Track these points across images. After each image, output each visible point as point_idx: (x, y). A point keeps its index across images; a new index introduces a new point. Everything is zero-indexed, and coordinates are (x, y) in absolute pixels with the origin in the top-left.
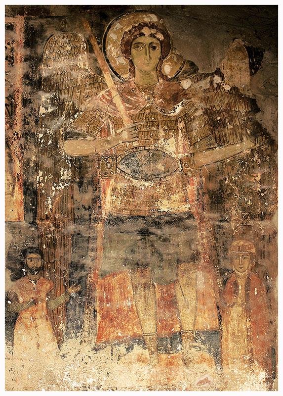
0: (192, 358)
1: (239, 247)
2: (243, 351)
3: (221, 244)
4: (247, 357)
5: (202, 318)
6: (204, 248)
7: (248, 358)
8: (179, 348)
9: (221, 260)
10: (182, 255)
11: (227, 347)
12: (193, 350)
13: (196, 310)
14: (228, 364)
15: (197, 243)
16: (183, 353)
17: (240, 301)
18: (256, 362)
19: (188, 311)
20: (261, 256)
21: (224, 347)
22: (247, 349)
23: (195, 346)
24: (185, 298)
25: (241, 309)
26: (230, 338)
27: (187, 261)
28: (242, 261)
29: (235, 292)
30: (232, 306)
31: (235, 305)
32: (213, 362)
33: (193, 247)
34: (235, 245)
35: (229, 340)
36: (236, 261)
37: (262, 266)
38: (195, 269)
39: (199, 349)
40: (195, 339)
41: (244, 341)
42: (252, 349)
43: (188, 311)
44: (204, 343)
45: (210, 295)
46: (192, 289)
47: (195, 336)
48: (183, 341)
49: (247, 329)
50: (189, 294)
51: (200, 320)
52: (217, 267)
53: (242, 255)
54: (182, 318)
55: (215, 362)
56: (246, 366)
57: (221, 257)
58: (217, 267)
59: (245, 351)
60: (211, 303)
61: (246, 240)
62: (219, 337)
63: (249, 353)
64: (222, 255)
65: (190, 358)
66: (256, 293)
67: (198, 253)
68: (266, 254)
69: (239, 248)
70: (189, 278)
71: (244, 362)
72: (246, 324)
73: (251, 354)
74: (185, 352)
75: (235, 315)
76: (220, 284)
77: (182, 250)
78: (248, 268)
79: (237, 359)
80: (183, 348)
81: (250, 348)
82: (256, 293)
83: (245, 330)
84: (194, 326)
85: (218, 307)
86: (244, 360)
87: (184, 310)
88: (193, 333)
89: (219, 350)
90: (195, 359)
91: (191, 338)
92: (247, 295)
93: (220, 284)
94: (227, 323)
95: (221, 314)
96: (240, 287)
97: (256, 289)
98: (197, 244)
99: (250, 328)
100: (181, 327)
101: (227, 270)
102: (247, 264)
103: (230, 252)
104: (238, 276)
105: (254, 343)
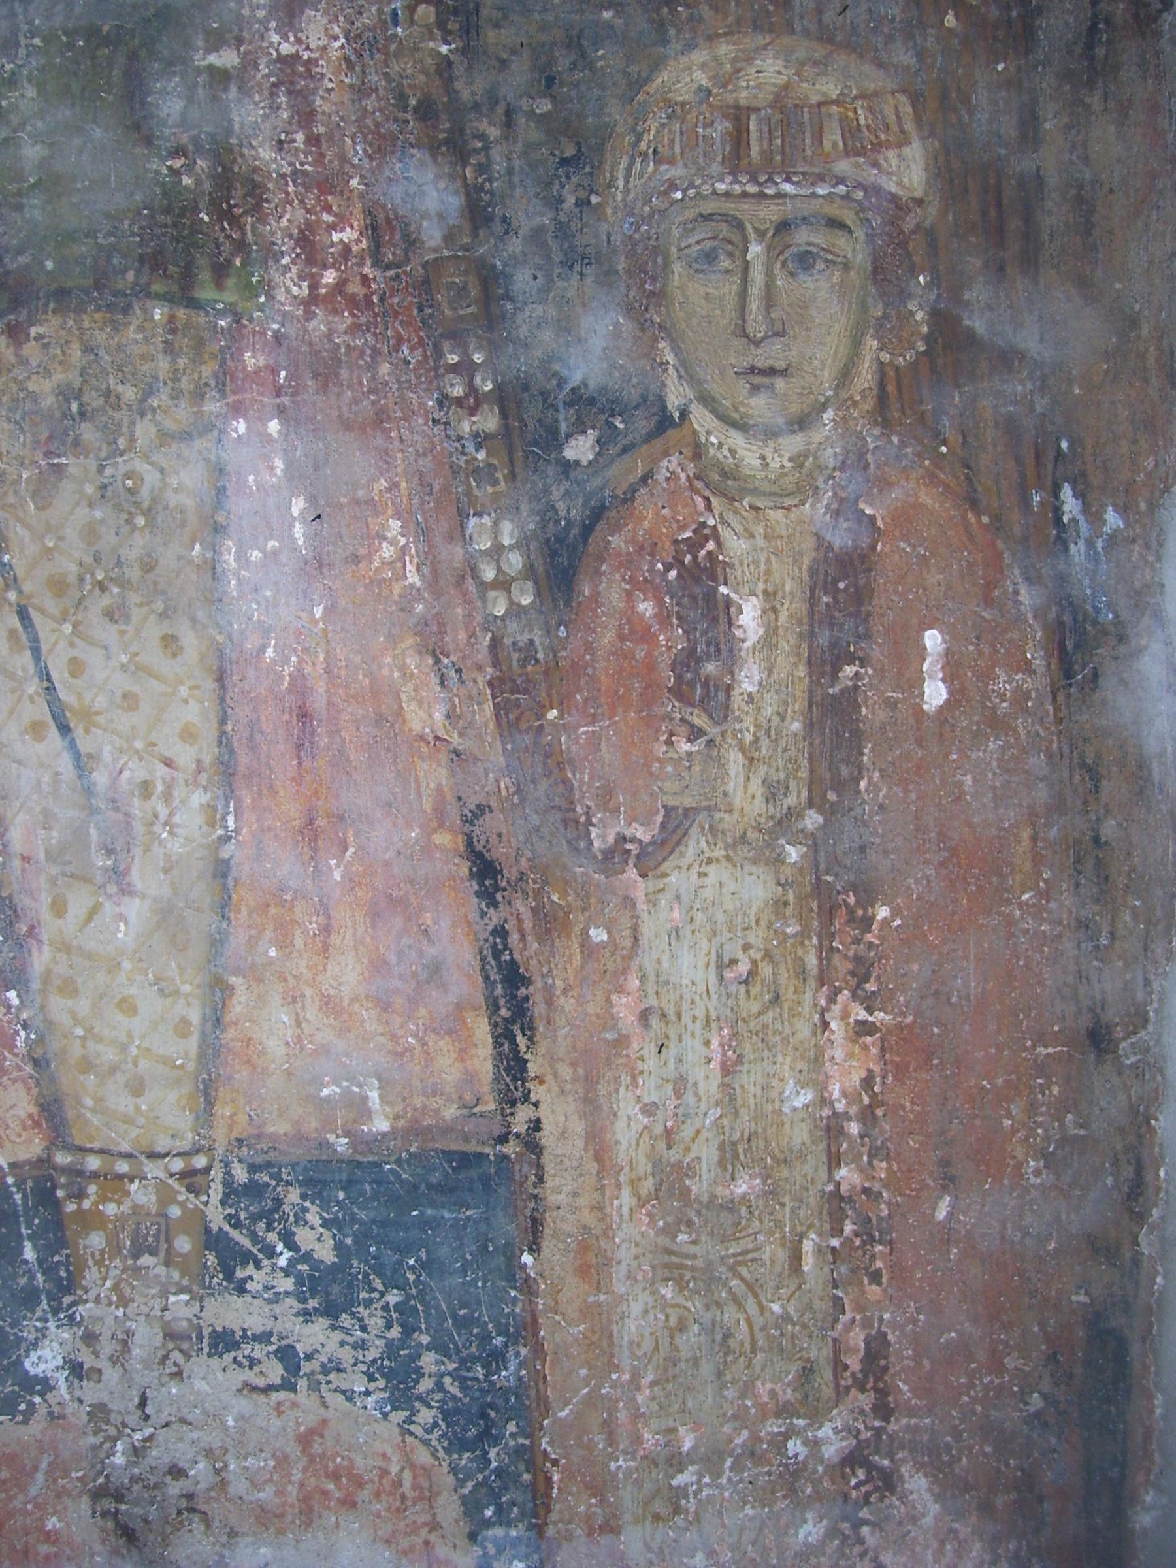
0: (201, 1470)
1: (739, 116)
2: (774, 1382)
3: (520, 72)
4: (826, 1431)
5: (293, 999)
6: (306, 117)
7: (832, 1451)
8: (44, 1361)
9: (523, 280)
10: (35, 209)
11: (601, 1345)
12: (211, 1380)
13: (224, 907)
14: (611, 1527)
15: (227, 58)
16: (99, 1412)
17: (744, 794)
18: (917, 1484)
19: (126, 923)
20: (997, 233)
21: (562, 1330)
22: (820, 1353)
23: (223, 1342)
24: (82, 763)
25: (755, 889)
26: (632, 1231)
27: (96, 290)
28: (769, 301)
29: (697, 684)
30: (649, 859)
31: (695, 844)
32: (449, 1509)
33: (170, 105)
34: (683, 93)
35: (625, 1254)
36: (699, 295)
37: (1007, 359)
38: (199, 395)
39: (275, 1372)
40: (227, 1260)
41: (796, 1257)
42: (876, 1350)
43: (126, 923)
44: (328, 1294)
45: (389, 720)
46: (170, 642)
47: (216, 1218)
48: (92, 1275)
49: (833, 1129)
50: (130, 701)
51: (271, 1026)
52: (466, 369)
53: (771, 213)
54: (59, 1007)
55: (471, 1507)
56: (811, 1530)
57: (515, 245)
58: (466, 369)
59: (807, 1372)
60: (397, 826)
61: (825, 36)
62: (507, 1228)
63: (841, 1393)
64: (528, 213)
65: (177, 1472)
66: (935, 694)
67: (236, 189)
68: (1054, 214)
69: (739, 138)
70: (128, 503)
71: (792, 1492)
72: (817, 1061)
73: (865, 1400)
74: (123, 1405)
75: (690, 968)
76: (503, 583)
77: (32, 153)
78: (845, 376)
79: (710, 1460)
80: (87, 1359)
81: (857, 1338)
82: (935, 694)
83: (800, 1134)
84: (207, 1095)
85: (486, 872)
86: (793, 1474)
87: (78, 905)
88: (193, 1180)
89: (506, 1376)
90: (239, 1486)
91: (183, 1244)
92: (835, 722)
93: (503, 583)
94: (600, 1062)
95: (527, 950)
96: (750, 618)
97: (933, 640)
98: (220, 77)
99: (867, 1116)
100: (52, 1115)
101: (590, 407)
102: (828, 331)
103: (627, 181)
104: (724, 483)
105: (900, 1274)
